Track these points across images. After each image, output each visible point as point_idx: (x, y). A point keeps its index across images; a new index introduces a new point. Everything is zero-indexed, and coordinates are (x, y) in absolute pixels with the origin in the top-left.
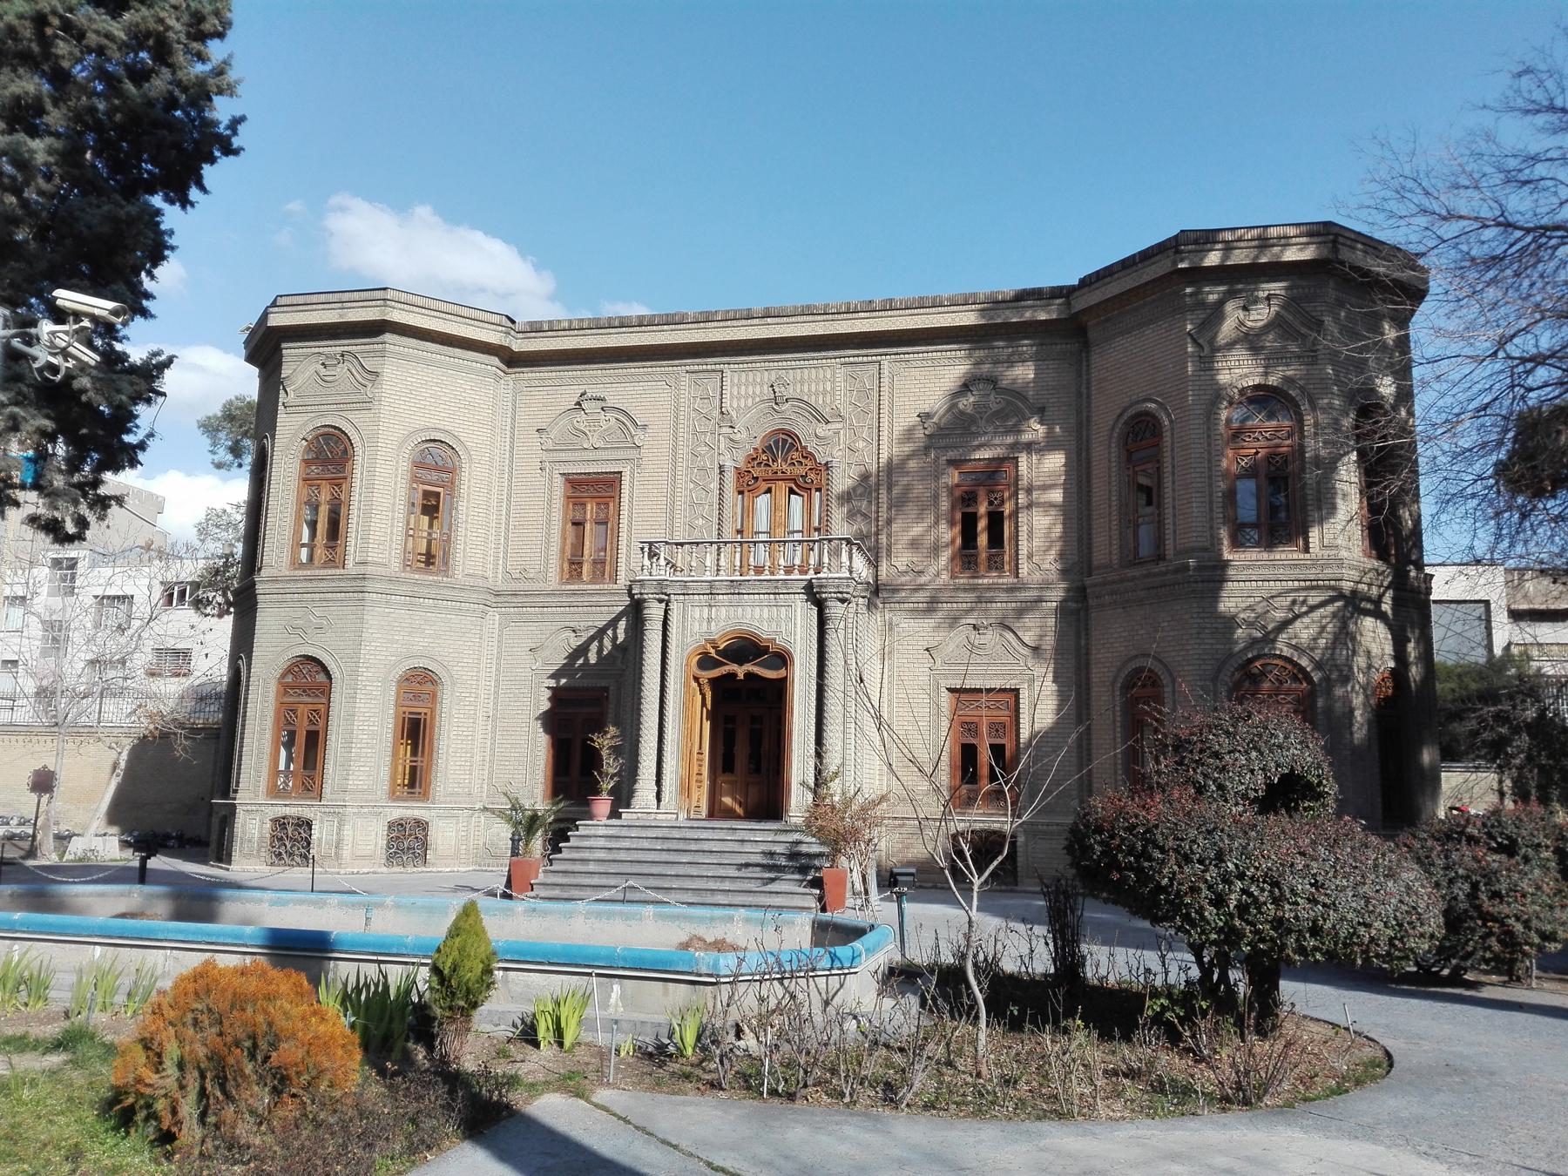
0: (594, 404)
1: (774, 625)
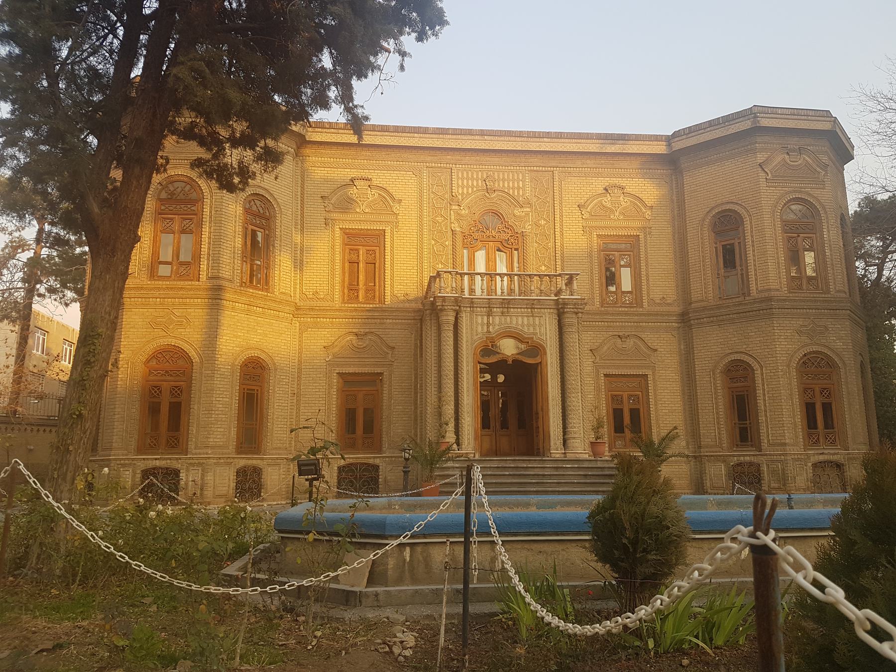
0: (362, 182)
1: (531, 329)
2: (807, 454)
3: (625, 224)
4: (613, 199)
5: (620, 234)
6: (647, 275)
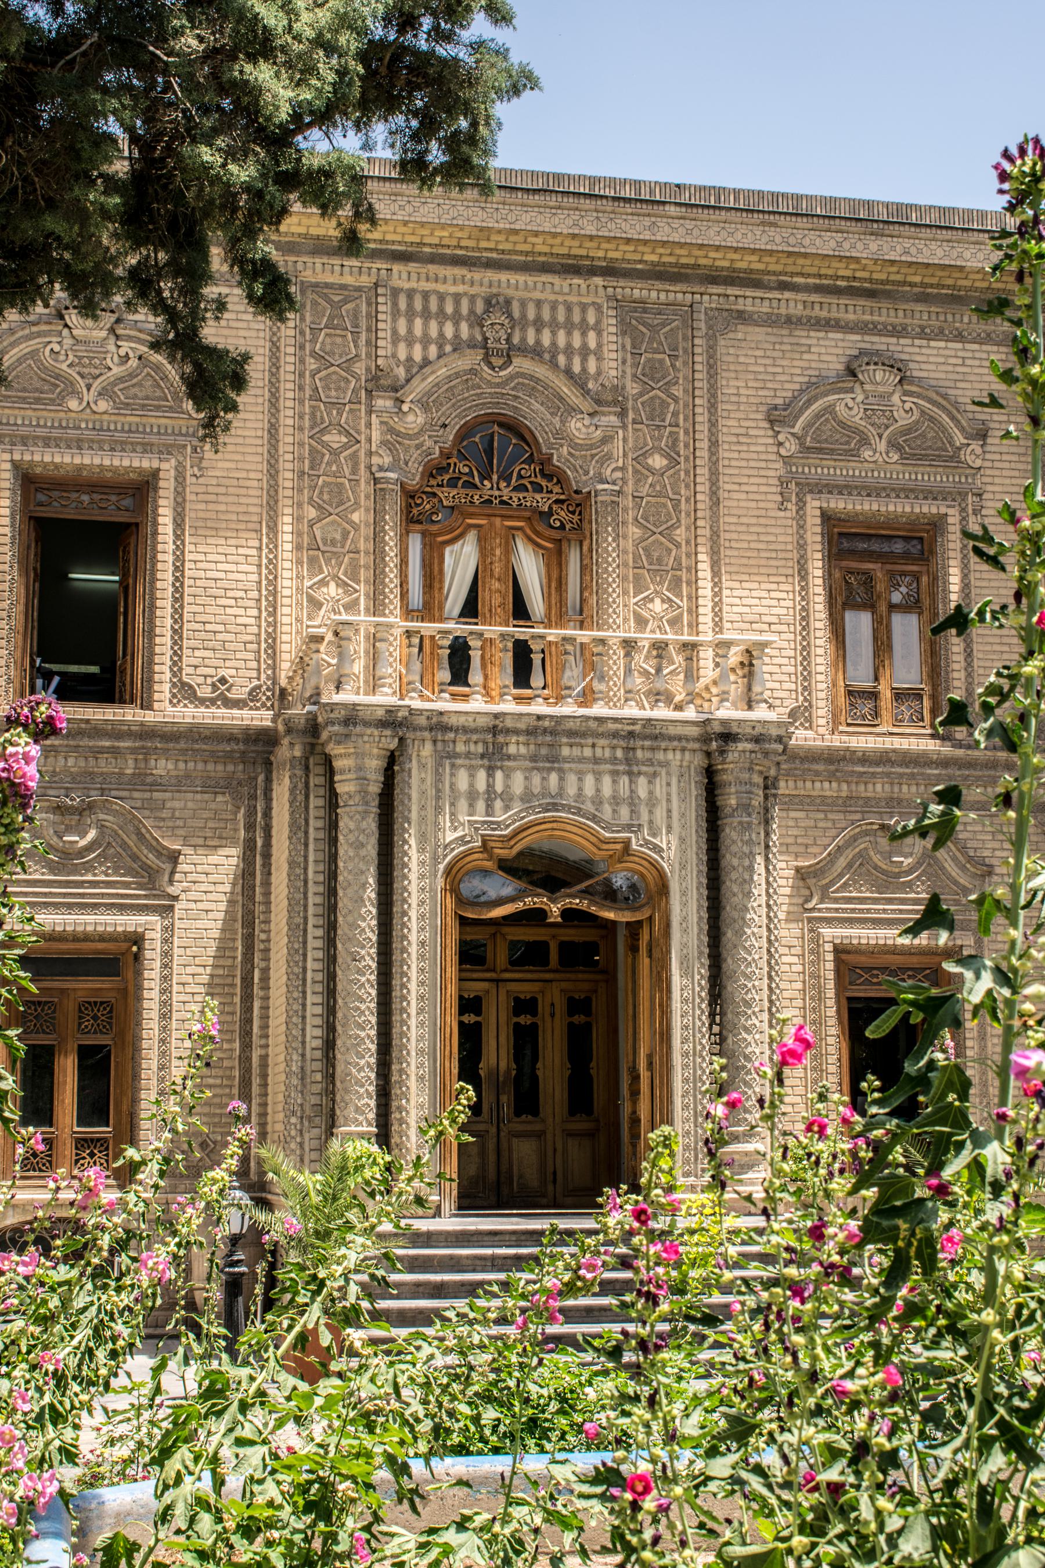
1: (624, 812)
4: (871, 400)
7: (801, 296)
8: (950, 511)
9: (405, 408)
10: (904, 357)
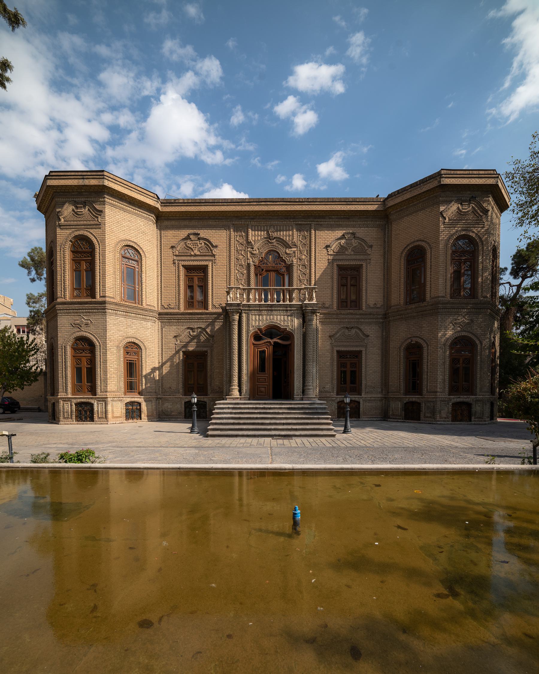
2: (449, 398)
3: (355, 257)
4: (348, 241)
5: (351, 264)
6: (366, 290)
7: (334, 220)
8: (364, 264)
9: (254, 250)
10: (355, 232)
